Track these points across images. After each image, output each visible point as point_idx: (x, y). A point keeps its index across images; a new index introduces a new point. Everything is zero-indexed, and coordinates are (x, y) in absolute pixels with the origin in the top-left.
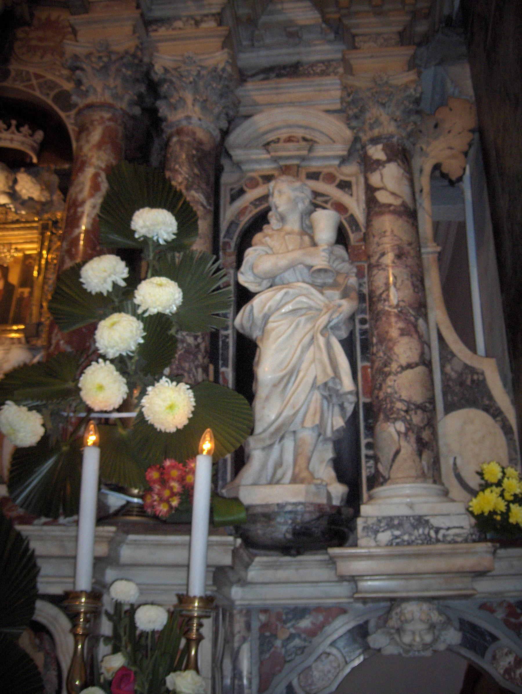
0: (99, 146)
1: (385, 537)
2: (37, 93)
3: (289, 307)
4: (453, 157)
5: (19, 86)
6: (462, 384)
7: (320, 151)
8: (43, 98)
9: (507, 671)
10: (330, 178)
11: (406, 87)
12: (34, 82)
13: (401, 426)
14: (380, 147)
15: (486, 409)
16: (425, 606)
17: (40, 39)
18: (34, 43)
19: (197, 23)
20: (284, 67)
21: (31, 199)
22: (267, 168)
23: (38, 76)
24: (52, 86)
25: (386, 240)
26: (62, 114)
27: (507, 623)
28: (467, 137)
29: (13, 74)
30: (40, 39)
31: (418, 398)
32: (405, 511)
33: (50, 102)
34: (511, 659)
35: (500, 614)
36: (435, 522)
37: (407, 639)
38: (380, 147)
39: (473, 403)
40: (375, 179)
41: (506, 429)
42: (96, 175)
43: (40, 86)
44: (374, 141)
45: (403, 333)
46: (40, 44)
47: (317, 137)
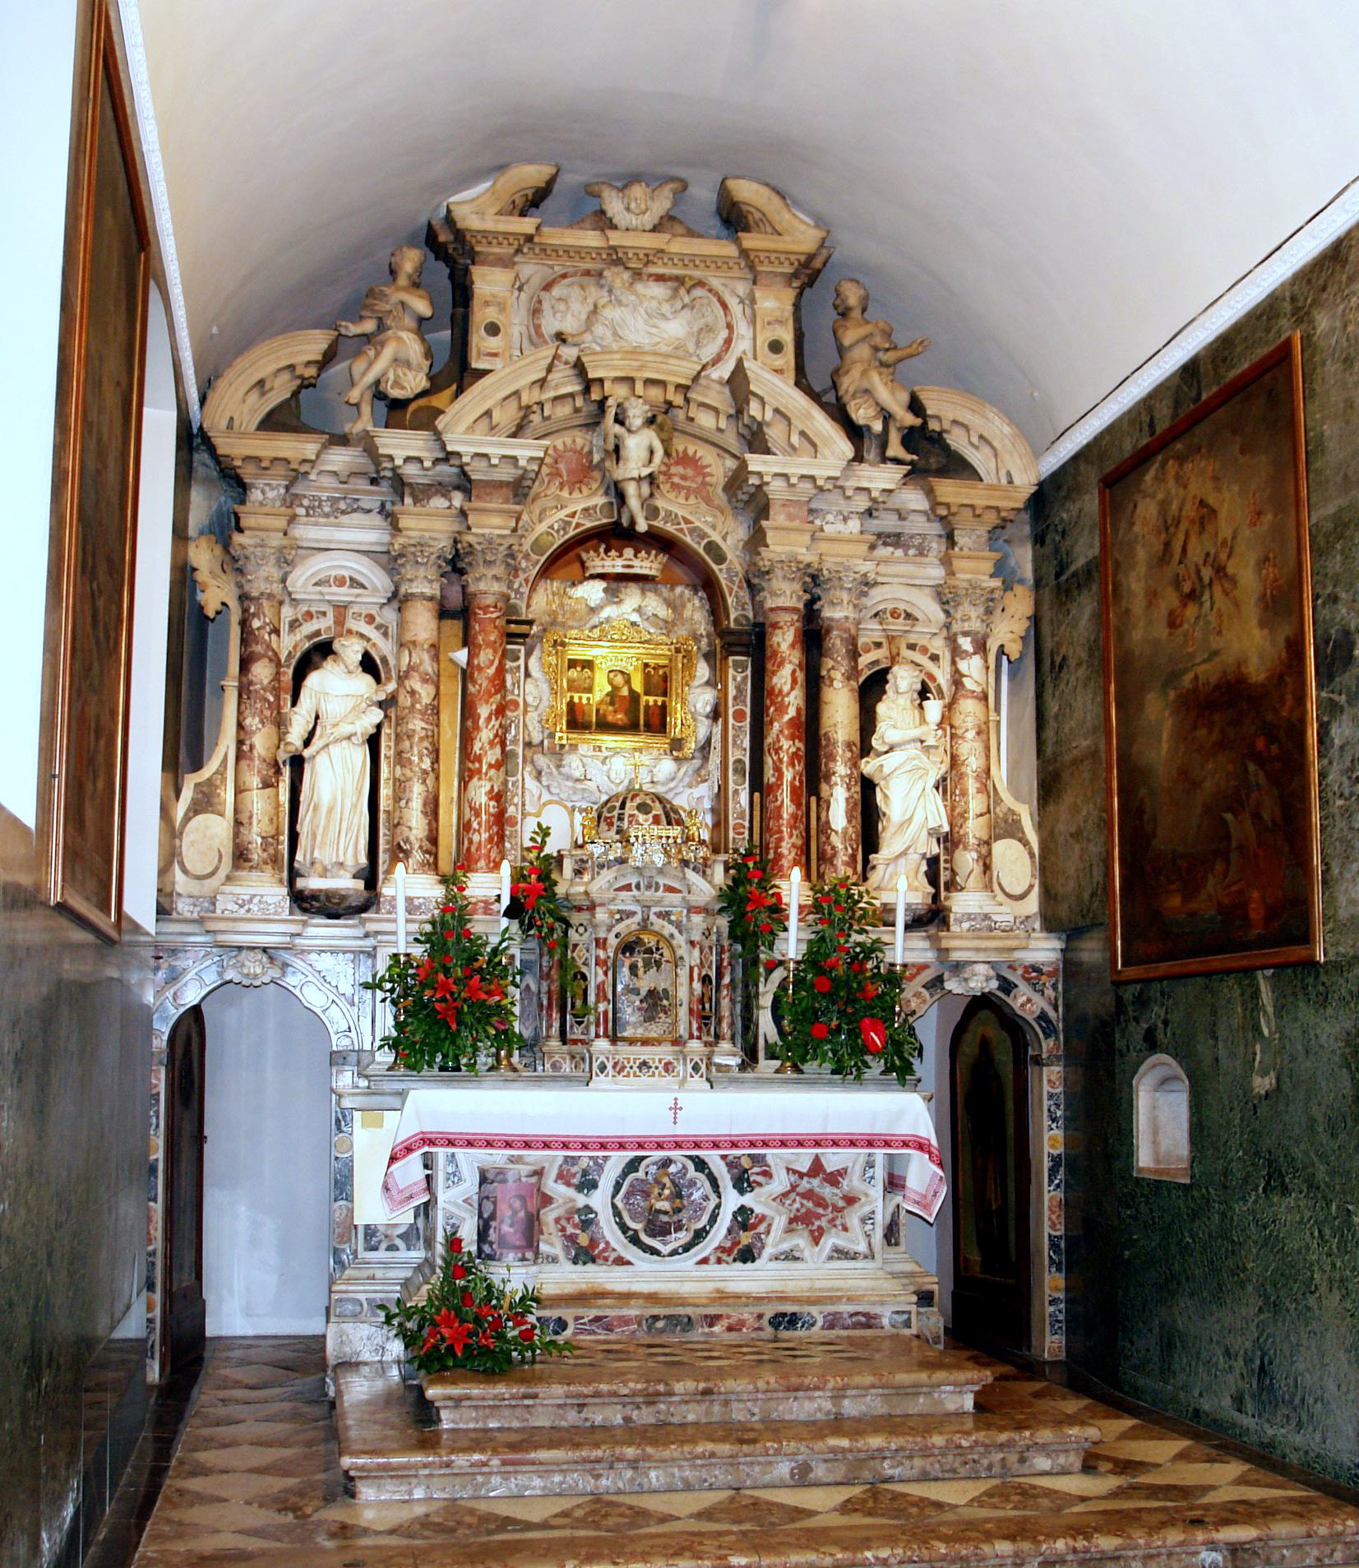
0: (793, 646)
1: (966, 925)
2: (688, 539)
3: (908, 768)
4: (1014, 641)
5: (670, 528)
6: (1006, 821)
7: (918, 629)
8: (695, 546)
9: (1022, 1005)
10: (924, 650)
11: (992, 591)
12: (683, 526)
13: (974, 855)
14: (969, 639)
15: (1020, 840)
16: (987, 966)
17: (684, 478)
18: (676, 480)
19: (845, 520)
20: (889, 536)
21: (655, 615)
22: (878, 637)
23: (687, 521)
24: (703, 535)
25: (969, 719)
26: (715, 567)
27: (1023, 977)
28: (1026, 624)
29: (662, 514)
30: (684, 478)
31: (985, 838)
32: (978, 911)
33: (701, 551)
34: (1024, 998)
35: (1020, 972)
36: (995, 918)
37: (972, 985)
38: (969, 639)
39: (1011, 836)
40: (963, 666)
41: (1031, 854)
42: (794, 672)
43: (692, 531)
44: (965, 634)
45: (979, 791)
46: (683, 483)
47: (916, 613)
